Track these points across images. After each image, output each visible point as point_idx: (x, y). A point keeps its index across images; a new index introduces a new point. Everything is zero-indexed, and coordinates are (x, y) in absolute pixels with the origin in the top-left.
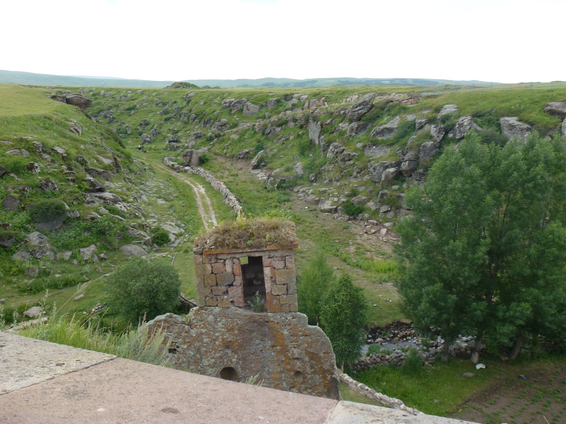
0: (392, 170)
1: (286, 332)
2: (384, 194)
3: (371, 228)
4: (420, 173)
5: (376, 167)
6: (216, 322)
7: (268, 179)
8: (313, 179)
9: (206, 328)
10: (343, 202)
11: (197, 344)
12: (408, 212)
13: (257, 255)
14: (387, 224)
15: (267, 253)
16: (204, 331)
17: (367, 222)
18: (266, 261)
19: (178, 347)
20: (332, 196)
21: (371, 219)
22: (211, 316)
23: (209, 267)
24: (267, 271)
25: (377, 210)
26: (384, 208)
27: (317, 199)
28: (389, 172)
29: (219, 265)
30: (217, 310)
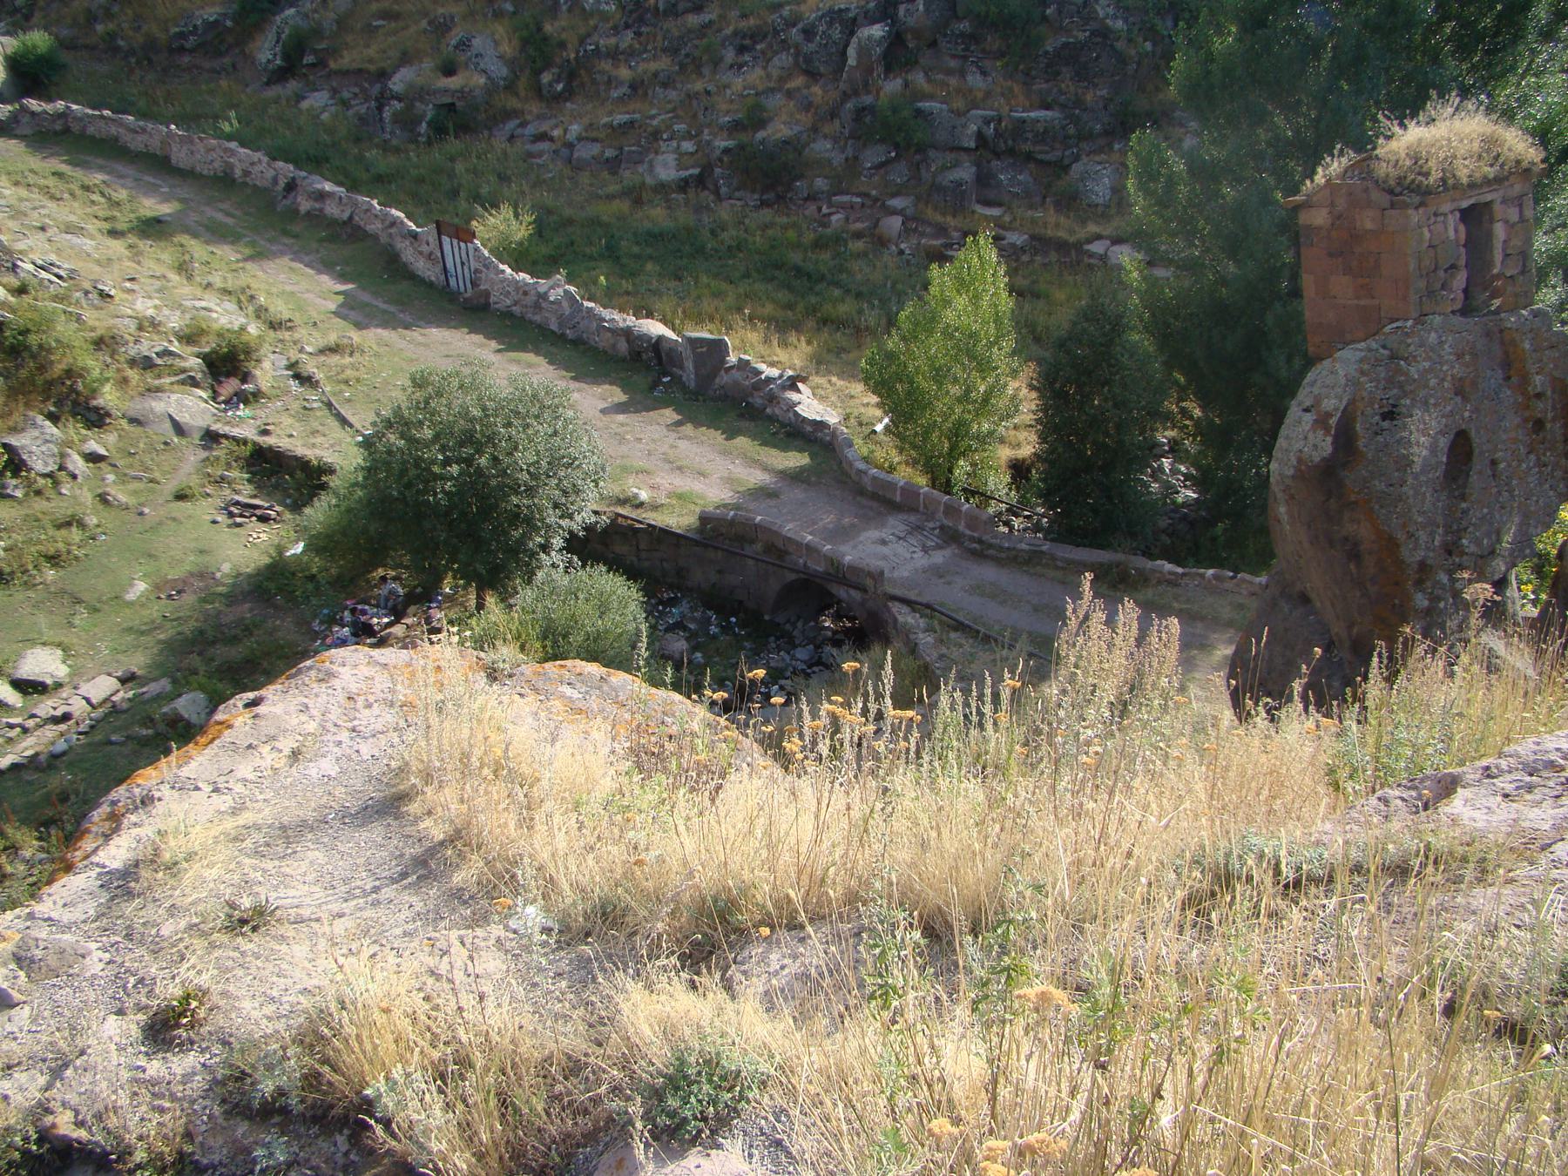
0: (877, 31)
1: (1527, 346)
2: (864, 109)
3: (847, 219)
4: (962, 35)
5: (813, 26)
6: (1441, 343)
7: (380, 109)
8: (560, 87)
9: (1429, 358)
10: (726, 151)
11: (1422, 393)
12: (950, 156)
13: (1489, 197)
14: (897, 203)
15: (1501, 192)
16: (1427, 364)
17: (830, 205)
18: (1497, 207)
19: (1394, 406)
20: (671, 139)
21: (842, 193)
22: (1433, 335)
23: (1427, 235)
24: (1499, 231)
25: (853, 163)
26: (873, 156)
27: (609, 153)
28: (870, 38)
29: (1440, 227)
30: (1438, 319)
